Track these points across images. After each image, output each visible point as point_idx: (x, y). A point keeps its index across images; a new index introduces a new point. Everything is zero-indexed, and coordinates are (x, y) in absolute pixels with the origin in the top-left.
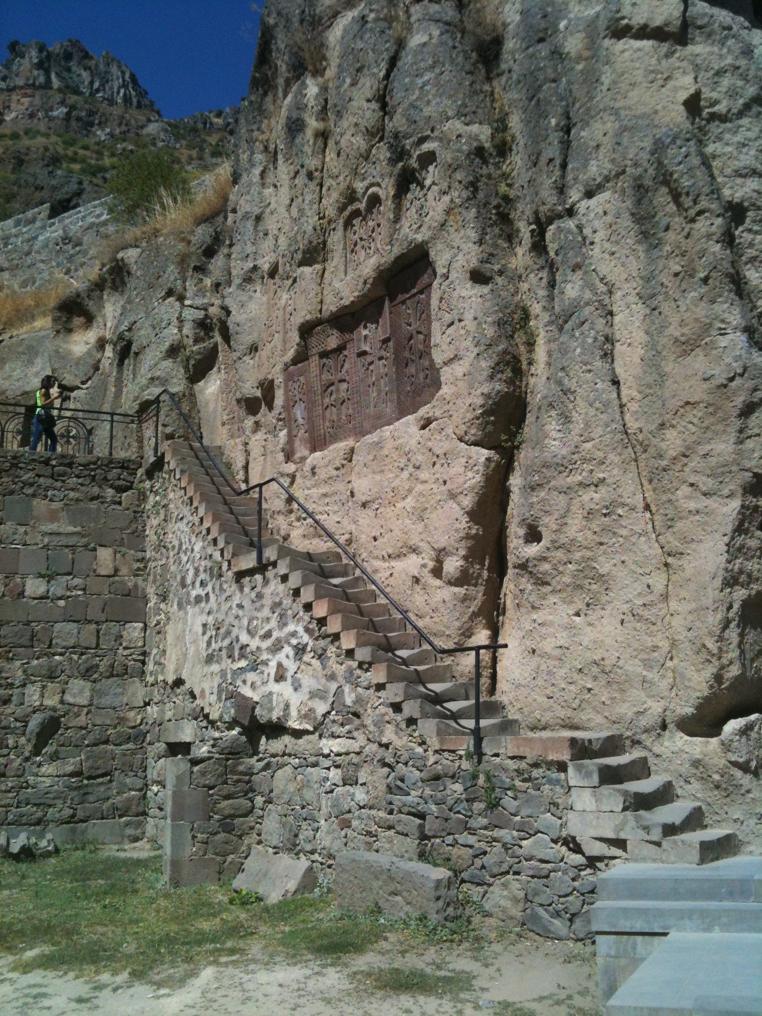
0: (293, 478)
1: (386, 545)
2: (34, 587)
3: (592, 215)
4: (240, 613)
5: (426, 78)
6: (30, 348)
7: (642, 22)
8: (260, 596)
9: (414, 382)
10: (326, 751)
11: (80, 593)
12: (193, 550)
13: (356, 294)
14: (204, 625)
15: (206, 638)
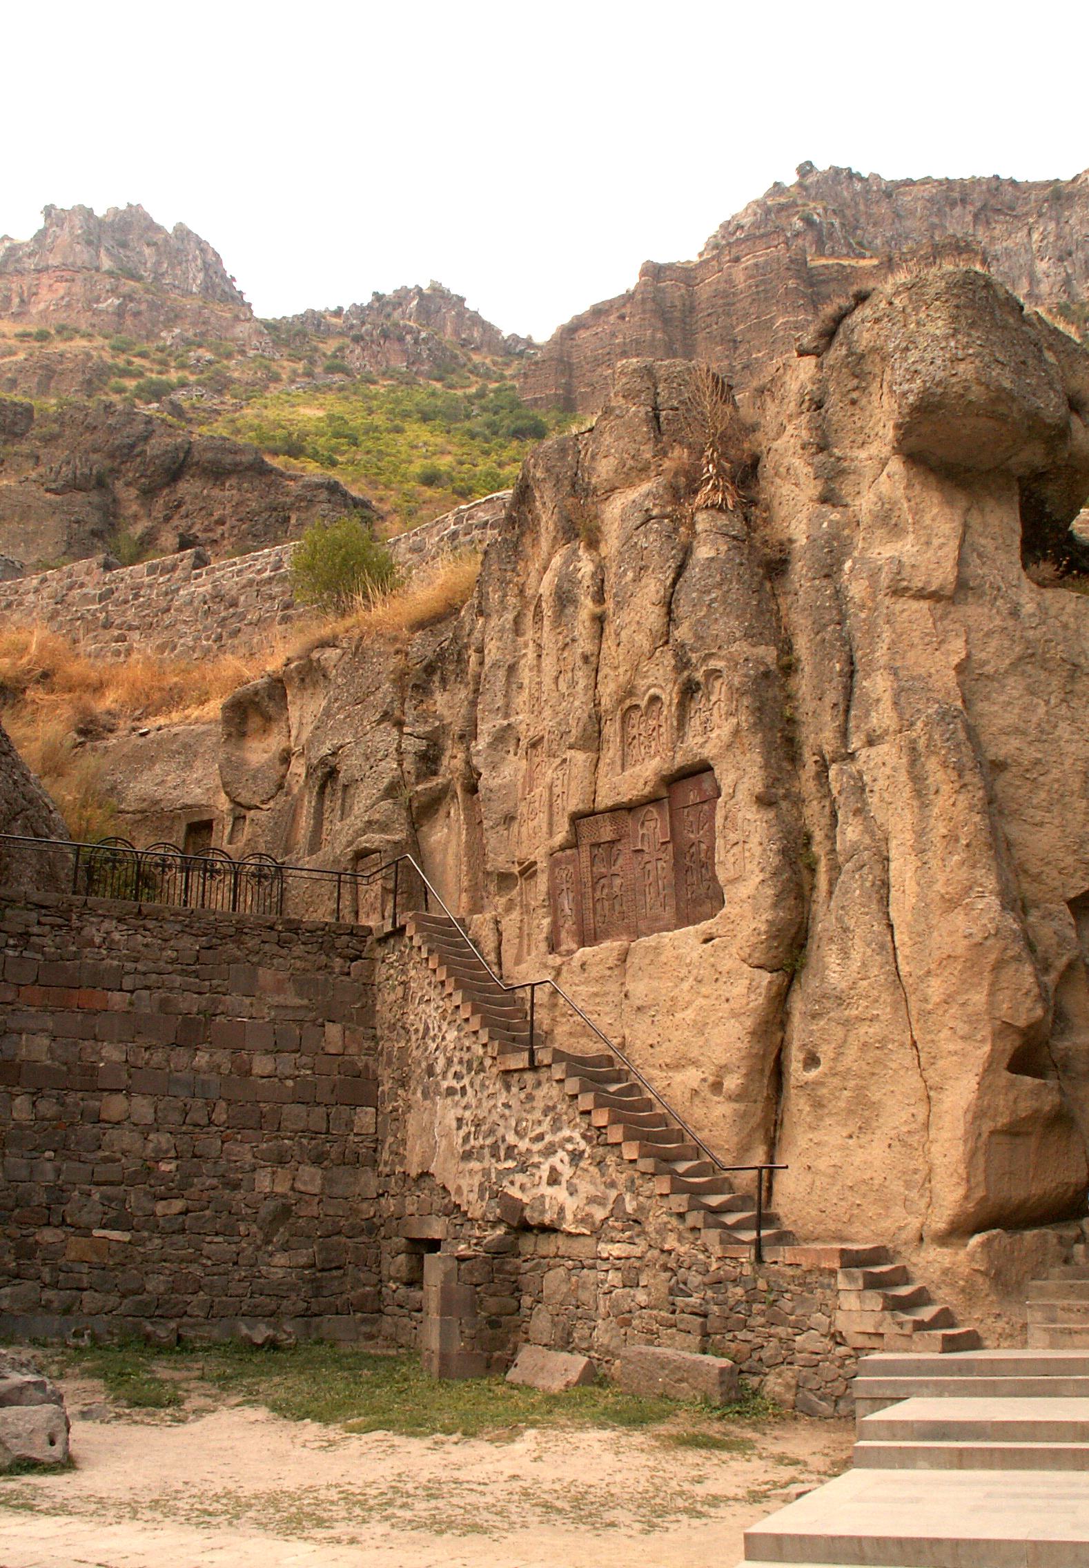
0: (558, 971)
1: (666, 1054)
2: (262, 1065)
3: (872, 764)
4: (507, 1112)
5: (714, 595)
6: (186, 746)
7: (920, 585)
8: (530, 1098)
9: (696, 895)
10: (605, 1255)
11: (308, 1072)
12: (444, 1038)
13: (635, 793)
14: (459, 1120)
15: (462, 1133)
